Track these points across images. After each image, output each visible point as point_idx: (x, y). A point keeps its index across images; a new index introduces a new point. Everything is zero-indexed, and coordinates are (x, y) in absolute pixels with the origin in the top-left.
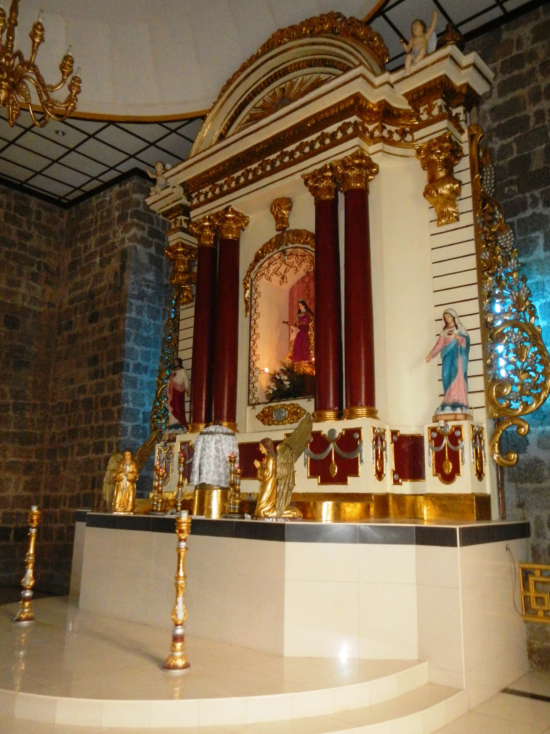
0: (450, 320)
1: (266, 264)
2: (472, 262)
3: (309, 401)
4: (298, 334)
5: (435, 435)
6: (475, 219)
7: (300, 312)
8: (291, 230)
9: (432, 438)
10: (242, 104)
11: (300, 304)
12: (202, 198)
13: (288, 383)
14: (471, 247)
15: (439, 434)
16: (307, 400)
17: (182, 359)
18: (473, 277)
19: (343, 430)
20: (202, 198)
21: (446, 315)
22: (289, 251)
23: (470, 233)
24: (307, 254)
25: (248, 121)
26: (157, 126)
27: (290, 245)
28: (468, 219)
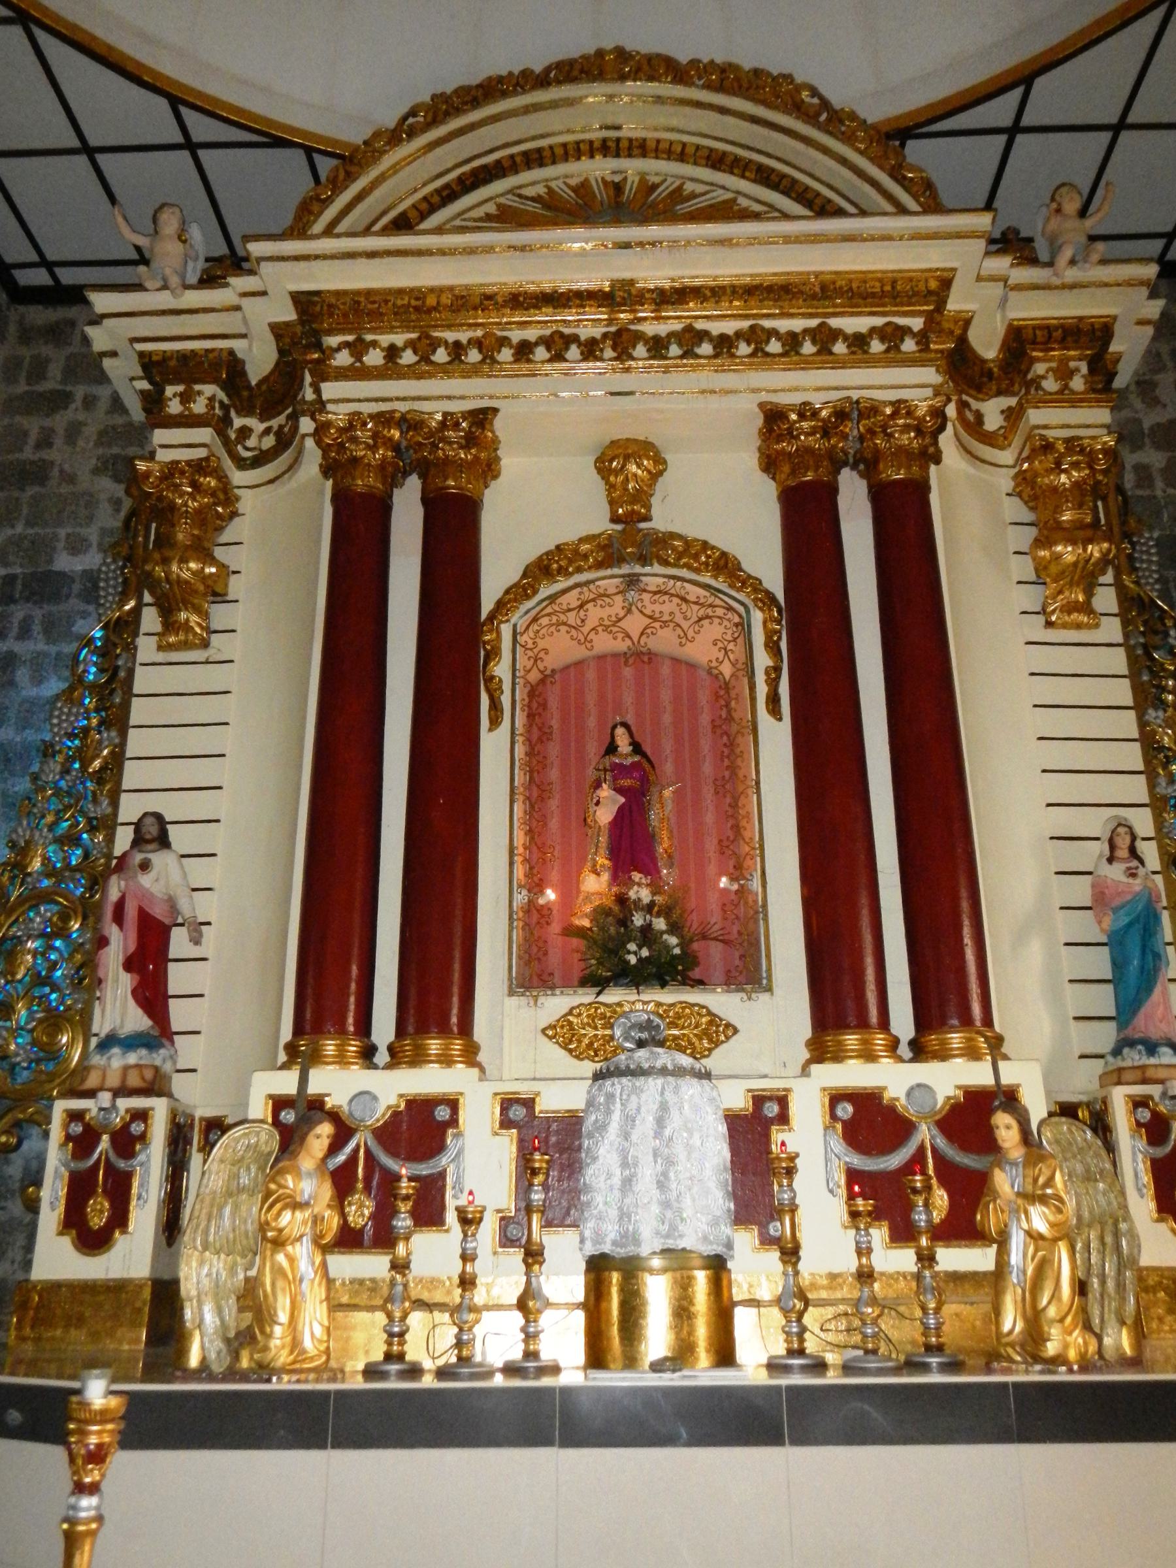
0: (1123, 842)
1: (572, 599)
2: (1128, 723)
3: (750, 999)
4: (622, 814)
5: (1145, 1115)
6: (1126, 636)
7: (612, 749)
8: (656, 532)
9: (1139, 1124)
10: (484, 167)
11: (620, 731)
12: (374, 358)
13: (673, 940)
14: (1123, 692)
15: (1156, 1115)
16: (743, 995)
17: (167, 819)
18: (1133, 757)
19: (959, 1087)
20: (374, 358)
21: (1121, 830)
22: (653, 583)
23: (1118, 660)
24: (718, 602)
25: (489, 217)
26: (163, 104)
27: (657, 568)
28: (1112, 629)
